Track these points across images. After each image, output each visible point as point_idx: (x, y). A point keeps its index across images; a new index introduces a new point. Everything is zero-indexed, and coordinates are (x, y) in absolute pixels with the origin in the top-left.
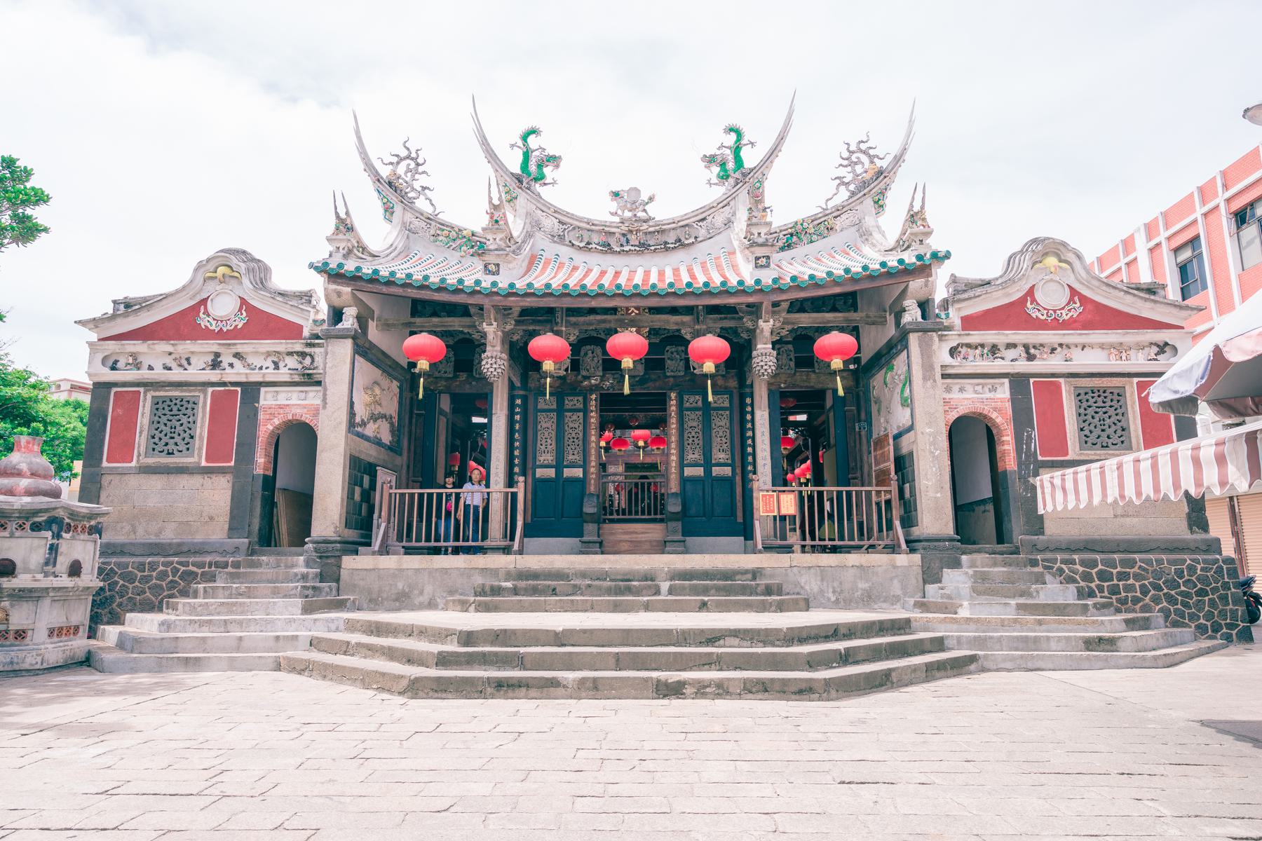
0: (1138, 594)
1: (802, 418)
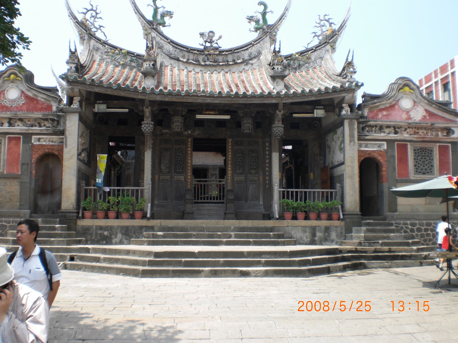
0: (431, 238)
1: (290, 147)
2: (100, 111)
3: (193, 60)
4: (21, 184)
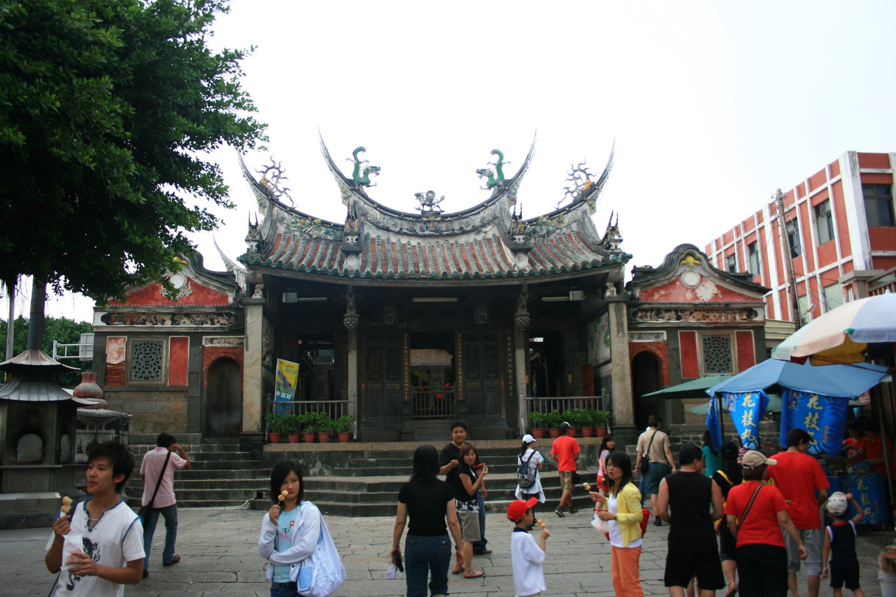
1: (540, 340)
2: (289, 301)
4: (189, 399)
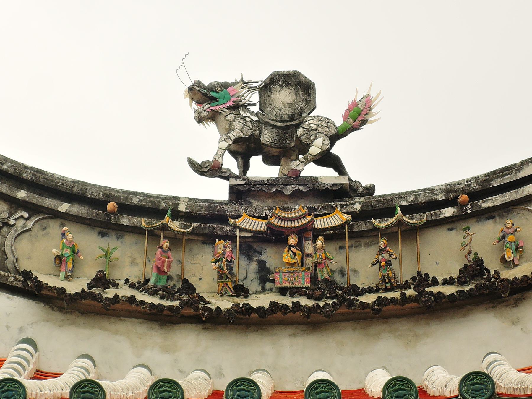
3: (142, 286)
